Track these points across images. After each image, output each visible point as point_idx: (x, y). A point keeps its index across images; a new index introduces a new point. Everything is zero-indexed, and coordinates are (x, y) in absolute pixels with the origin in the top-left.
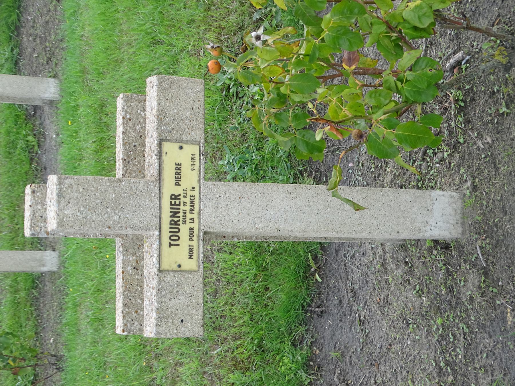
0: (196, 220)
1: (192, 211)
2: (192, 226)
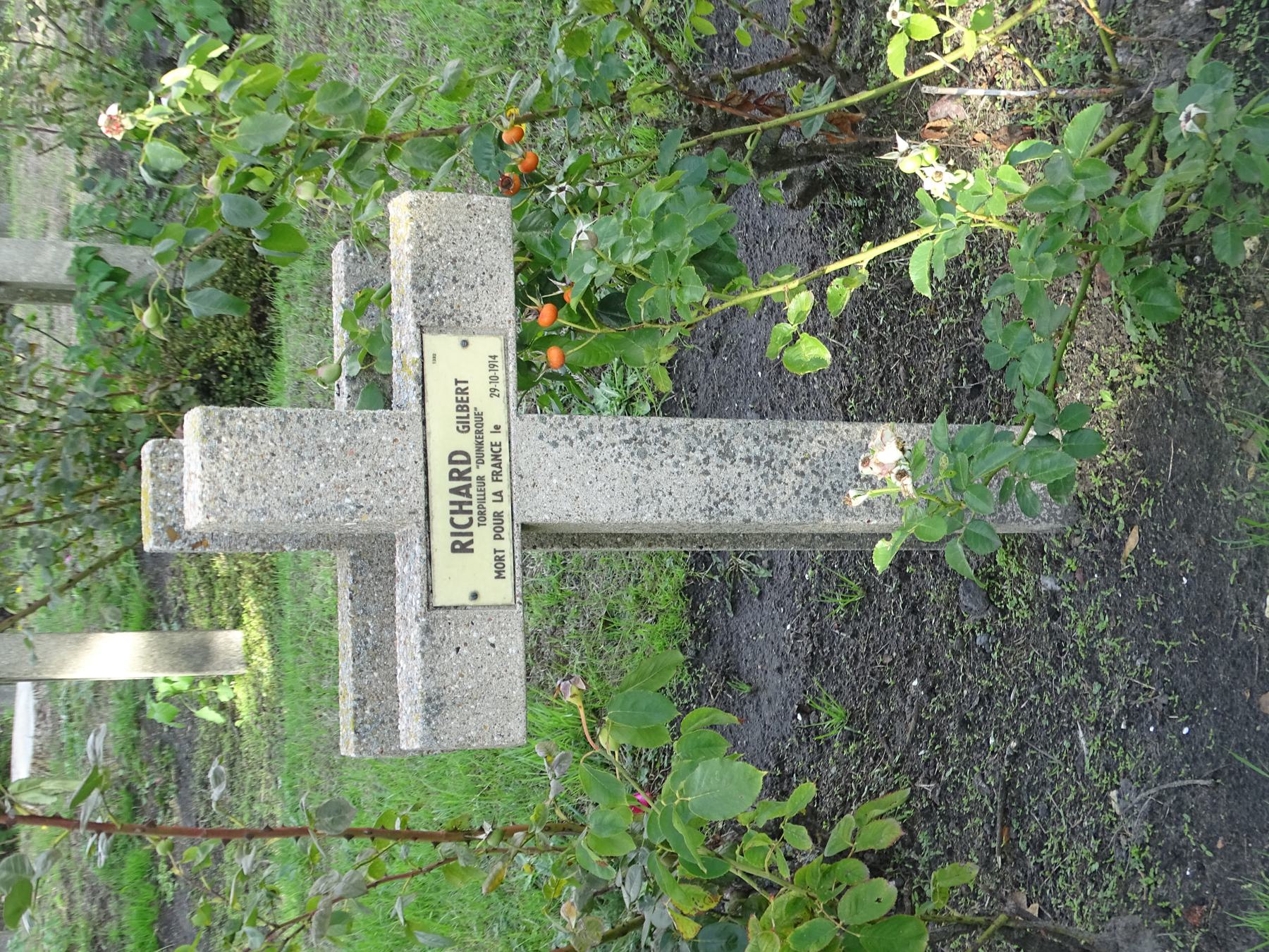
0: (506, 494)
1: (496, 476)
2: (499, 507)
